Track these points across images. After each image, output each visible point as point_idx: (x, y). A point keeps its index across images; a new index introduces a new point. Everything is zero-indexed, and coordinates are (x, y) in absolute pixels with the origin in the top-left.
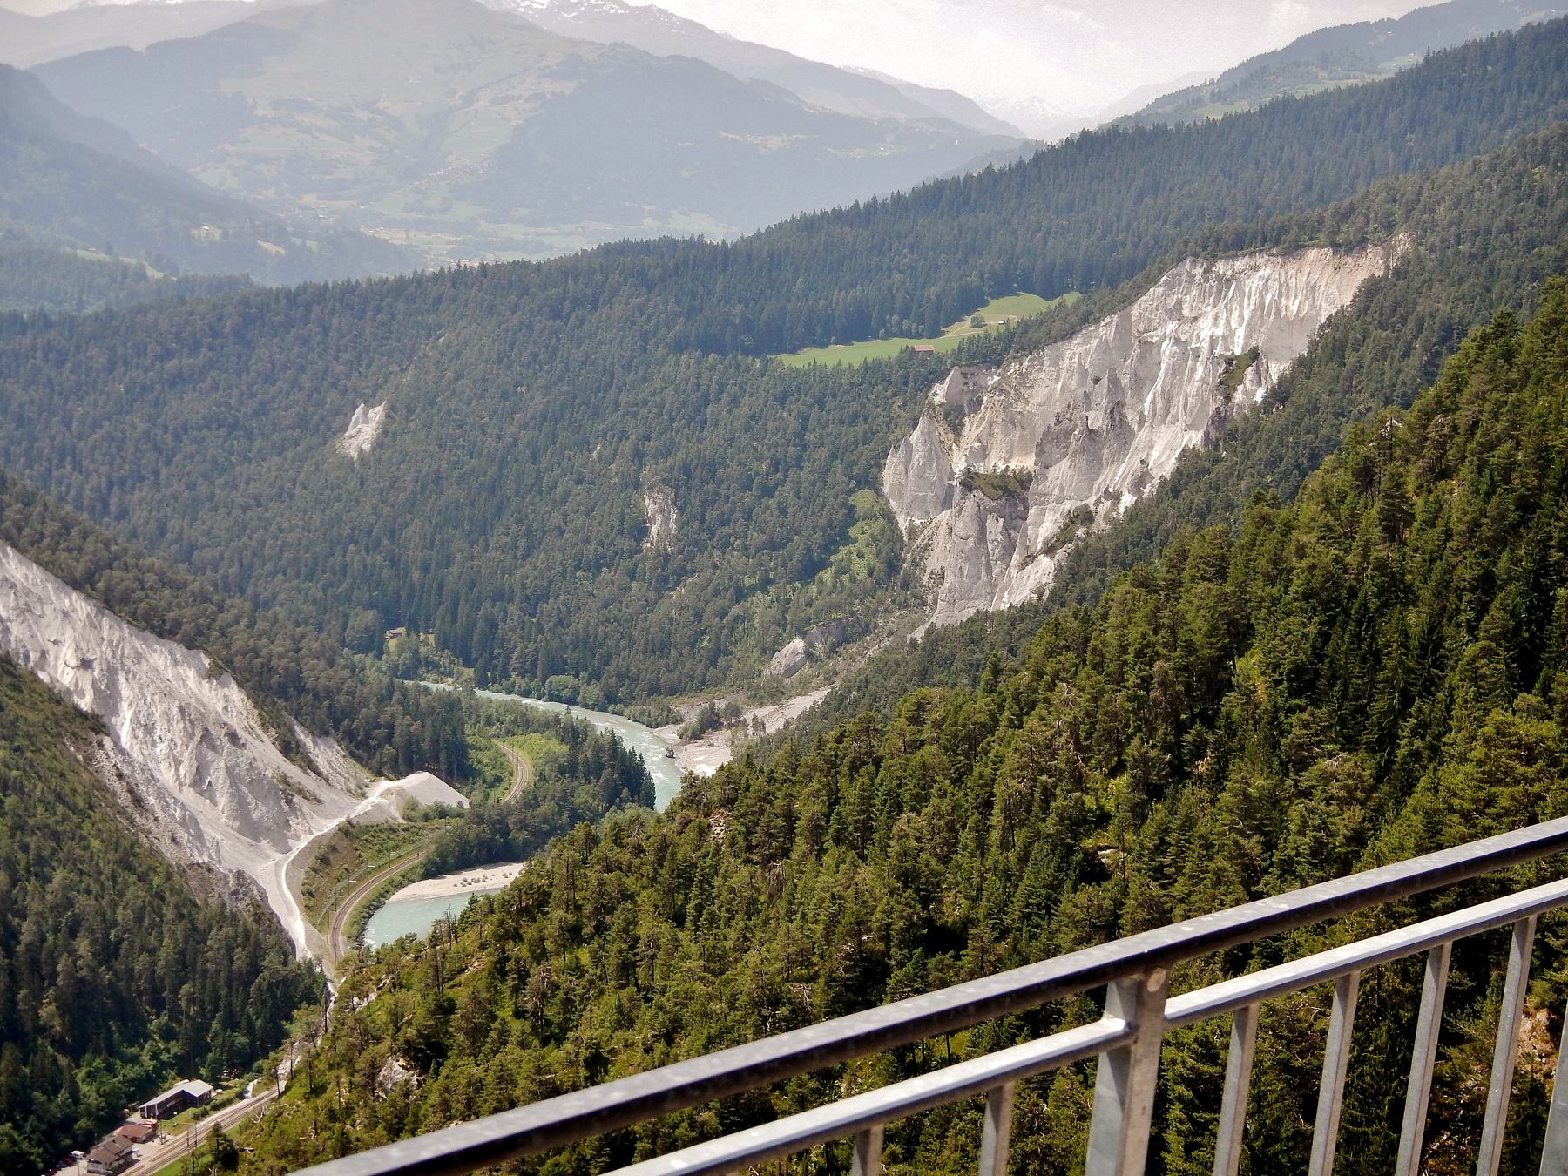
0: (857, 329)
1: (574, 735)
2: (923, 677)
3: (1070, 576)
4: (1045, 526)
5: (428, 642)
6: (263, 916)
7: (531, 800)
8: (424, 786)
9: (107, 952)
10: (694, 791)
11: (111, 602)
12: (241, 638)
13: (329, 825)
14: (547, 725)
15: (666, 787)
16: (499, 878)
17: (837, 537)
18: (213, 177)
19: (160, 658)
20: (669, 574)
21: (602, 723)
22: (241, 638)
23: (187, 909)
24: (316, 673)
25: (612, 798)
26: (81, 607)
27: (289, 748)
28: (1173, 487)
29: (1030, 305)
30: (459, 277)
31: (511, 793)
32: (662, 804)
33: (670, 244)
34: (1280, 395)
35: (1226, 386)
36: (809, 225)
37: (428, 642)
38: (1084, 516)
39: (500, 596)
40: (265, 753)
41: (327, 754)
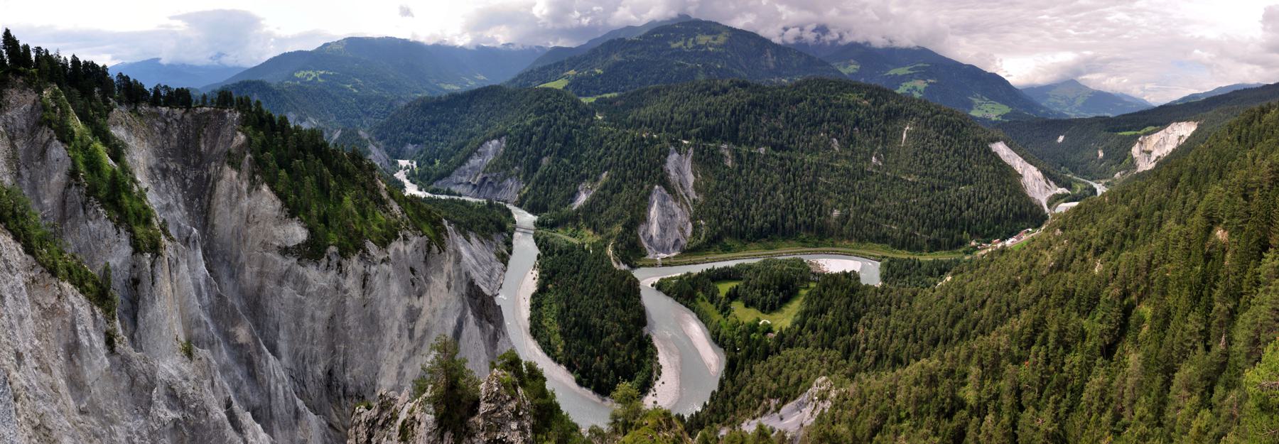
0: (1130, 130)
1: (1087, 184)
2: (1136, 179)
3: (1157, 166)
4: (1153, 158)
5: (1067, 169)
6: (1041, 206)
7: (1080, 193)
8: (1065, 191)
9: (1020, 208)
10: (1103, 194)
11: (1025, 159)
12: (1041, 166)
13: (1052, 194)
14: (1083, 182)
15: (1099, 192)
16: (1076, 204)
17: (1125, 158)
18: (1043, 104)
19: (1031, 167)
20: (1102, 161)
21: (1091, 183)
22: (1041, 166)
23: (1031, 203)
24: (1052, 172)
25: (1091, 194)
26: (1021, 159)
27: (1047, 182)
28: (1171, 153)
29: (1153, 128)
30: (1076, 119)
31: (1077, 192)
32: (1099, 195)
33: (1104, 117)
34: (1186, 141)
35: (1179, 139)
36: (1124, 115)
37: (1067, 169)
38: (1159, 157)
39: (1078, 163)
40: (1043, 182)
41: (1052, 183)
